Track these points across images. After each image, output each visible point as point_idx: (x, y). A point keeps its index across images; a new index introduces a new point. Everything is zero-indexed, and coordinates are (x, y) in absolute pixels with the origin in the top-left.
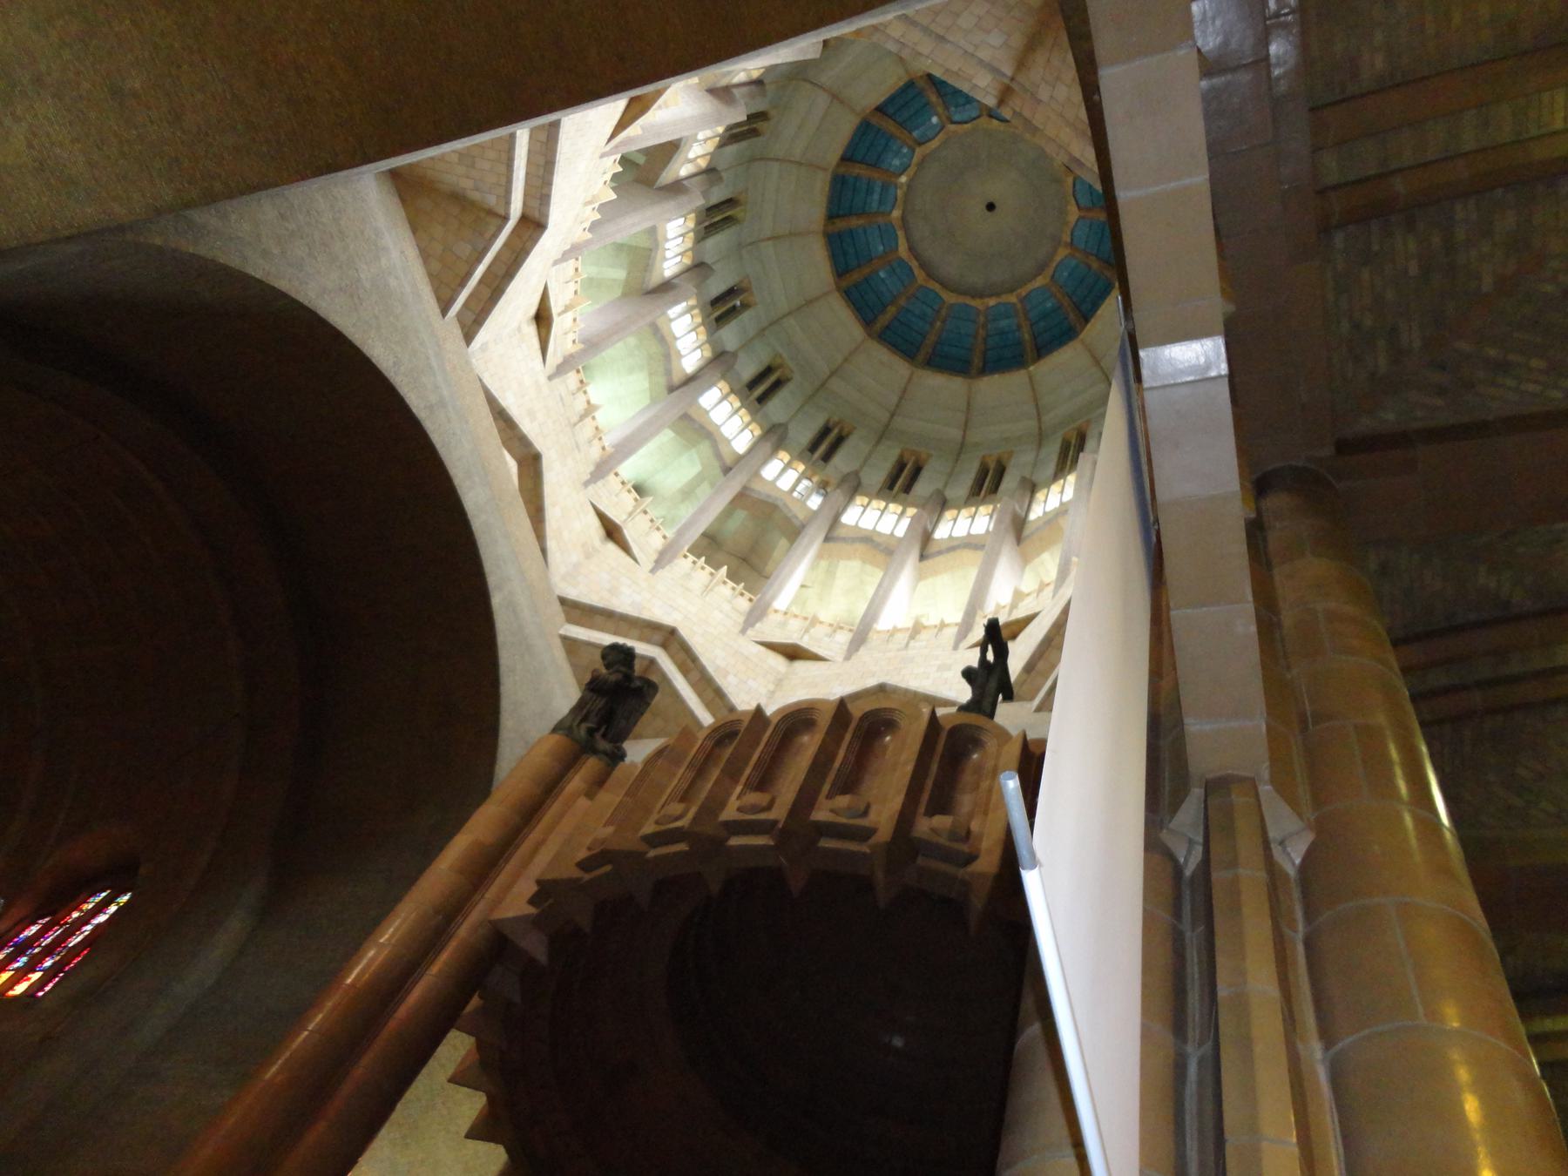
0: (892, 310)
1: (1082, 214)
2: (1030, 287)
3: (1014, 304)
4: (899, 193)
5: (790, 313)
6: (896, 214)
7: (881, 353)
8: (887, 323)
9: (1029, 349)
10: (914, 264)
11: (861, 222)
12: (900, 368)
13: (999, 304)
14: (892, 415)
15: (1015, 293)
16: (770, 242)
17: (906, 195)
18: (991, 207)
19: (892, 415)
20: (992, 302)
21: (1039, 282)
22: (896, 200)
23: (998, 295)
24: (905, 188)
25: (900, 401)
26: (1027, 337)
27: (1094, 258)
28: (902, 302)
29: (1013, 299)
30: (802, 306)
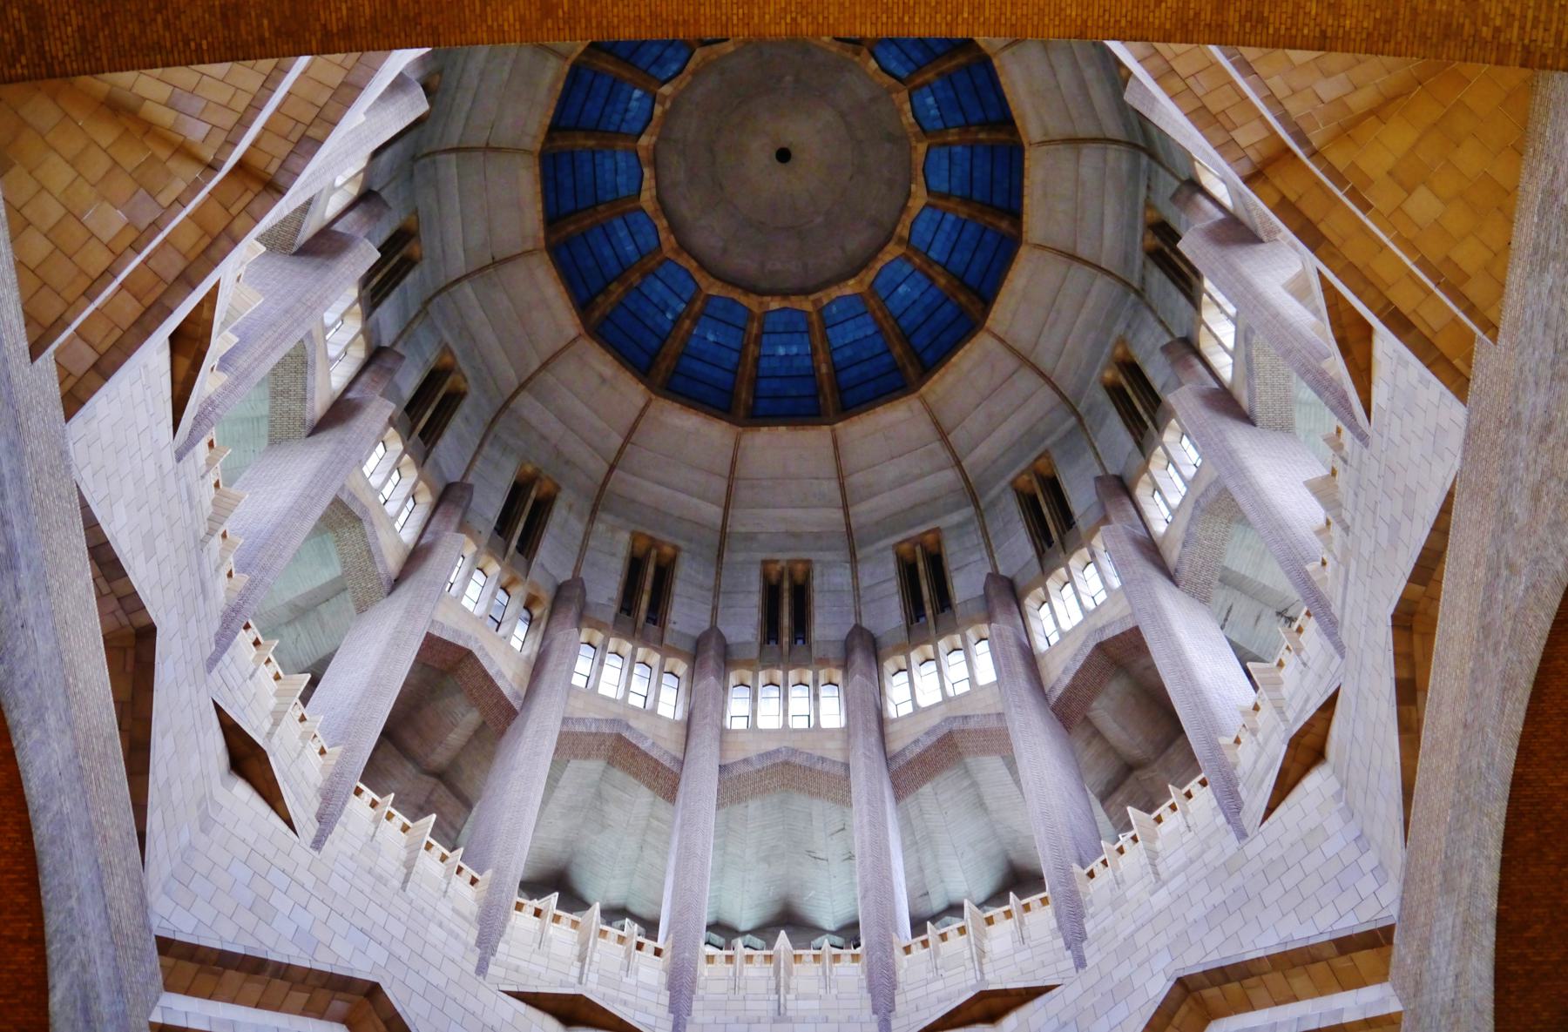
0: (617, 290)
1: (932, 201)
2: (835, 292)
3: (810, 313)
4: (658, 110)
5: (466, 276)
6: (645, 140)
7: (600, 362)
8: (609, 310)
9: (827, 389)
10: (662, 223)
11: (591, 143)
12: (631, 392)
13: (784, 309)
14: (612, 468)
15: (812, 297)
16: (453, 156)
17: (665, 114)
18: (784, 155)
19: (612, 468)
20: (775, 305)
21: (850, 287)
22: (650, 119)
23: (785, 294)
24: (668, 105)
25: (623, 446)
26: (824, 369)
27: (938, 269)
28: (635, 279)
29: (807, 305)
30: (487, 267)
